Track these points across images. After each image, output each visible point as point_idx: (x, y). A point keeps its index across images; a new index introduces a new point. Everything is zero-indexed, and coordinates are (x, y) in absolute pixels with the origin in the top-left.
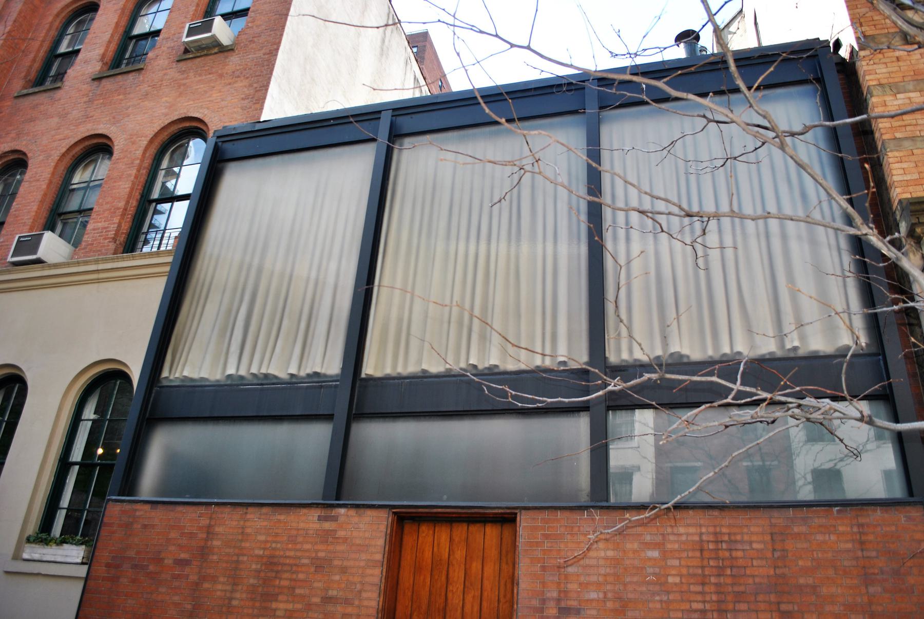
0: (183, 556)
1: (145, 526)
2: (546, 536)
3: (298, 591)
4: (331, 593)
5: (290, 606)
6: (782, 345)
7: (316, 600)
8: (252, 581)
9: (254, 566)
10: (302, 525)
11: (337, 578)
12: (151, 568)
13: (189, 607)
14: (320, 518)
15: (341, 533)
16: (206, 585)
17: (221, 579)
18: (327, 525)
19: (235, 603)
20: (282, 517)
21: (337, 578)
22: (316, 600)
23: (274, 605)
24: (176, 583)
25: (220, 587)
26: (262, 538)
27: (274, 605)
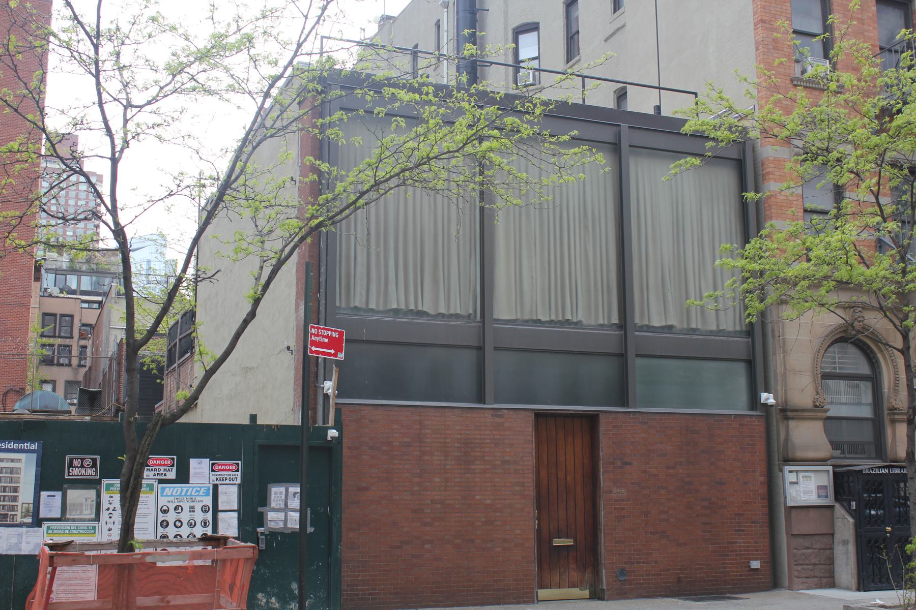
0: (406, 440)
1: (371, 421)
2: (614, 426)
3: (486, 458)
4: (507, 458)
5: (483, 467)
6: (718, 326)
7: (499, 463)
8: (457, 454)
9: (456, 445)
10: (482, 420)
11: (508, 450)
12: (384, 448)
13: (418, 471)
14: (492, 415)
15: (507, 425)
16: (426, 458)
17: (436, 453)
18: (497, 420)
19: (448, 467)
20: (469, 415)
21: (508, 450)
22: (499, 463)
23: (473, 467)
24: (406, 458)
25: (436, 458)
26: (459, 428)
27: (473, 467)
